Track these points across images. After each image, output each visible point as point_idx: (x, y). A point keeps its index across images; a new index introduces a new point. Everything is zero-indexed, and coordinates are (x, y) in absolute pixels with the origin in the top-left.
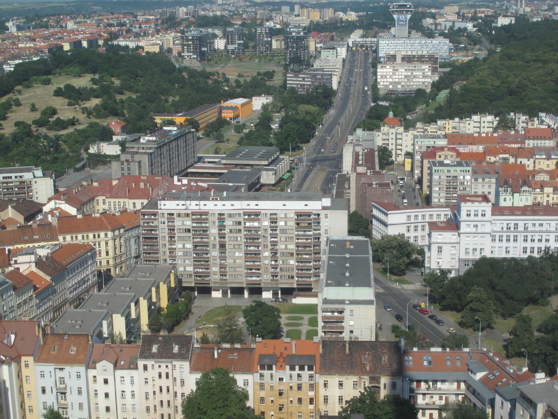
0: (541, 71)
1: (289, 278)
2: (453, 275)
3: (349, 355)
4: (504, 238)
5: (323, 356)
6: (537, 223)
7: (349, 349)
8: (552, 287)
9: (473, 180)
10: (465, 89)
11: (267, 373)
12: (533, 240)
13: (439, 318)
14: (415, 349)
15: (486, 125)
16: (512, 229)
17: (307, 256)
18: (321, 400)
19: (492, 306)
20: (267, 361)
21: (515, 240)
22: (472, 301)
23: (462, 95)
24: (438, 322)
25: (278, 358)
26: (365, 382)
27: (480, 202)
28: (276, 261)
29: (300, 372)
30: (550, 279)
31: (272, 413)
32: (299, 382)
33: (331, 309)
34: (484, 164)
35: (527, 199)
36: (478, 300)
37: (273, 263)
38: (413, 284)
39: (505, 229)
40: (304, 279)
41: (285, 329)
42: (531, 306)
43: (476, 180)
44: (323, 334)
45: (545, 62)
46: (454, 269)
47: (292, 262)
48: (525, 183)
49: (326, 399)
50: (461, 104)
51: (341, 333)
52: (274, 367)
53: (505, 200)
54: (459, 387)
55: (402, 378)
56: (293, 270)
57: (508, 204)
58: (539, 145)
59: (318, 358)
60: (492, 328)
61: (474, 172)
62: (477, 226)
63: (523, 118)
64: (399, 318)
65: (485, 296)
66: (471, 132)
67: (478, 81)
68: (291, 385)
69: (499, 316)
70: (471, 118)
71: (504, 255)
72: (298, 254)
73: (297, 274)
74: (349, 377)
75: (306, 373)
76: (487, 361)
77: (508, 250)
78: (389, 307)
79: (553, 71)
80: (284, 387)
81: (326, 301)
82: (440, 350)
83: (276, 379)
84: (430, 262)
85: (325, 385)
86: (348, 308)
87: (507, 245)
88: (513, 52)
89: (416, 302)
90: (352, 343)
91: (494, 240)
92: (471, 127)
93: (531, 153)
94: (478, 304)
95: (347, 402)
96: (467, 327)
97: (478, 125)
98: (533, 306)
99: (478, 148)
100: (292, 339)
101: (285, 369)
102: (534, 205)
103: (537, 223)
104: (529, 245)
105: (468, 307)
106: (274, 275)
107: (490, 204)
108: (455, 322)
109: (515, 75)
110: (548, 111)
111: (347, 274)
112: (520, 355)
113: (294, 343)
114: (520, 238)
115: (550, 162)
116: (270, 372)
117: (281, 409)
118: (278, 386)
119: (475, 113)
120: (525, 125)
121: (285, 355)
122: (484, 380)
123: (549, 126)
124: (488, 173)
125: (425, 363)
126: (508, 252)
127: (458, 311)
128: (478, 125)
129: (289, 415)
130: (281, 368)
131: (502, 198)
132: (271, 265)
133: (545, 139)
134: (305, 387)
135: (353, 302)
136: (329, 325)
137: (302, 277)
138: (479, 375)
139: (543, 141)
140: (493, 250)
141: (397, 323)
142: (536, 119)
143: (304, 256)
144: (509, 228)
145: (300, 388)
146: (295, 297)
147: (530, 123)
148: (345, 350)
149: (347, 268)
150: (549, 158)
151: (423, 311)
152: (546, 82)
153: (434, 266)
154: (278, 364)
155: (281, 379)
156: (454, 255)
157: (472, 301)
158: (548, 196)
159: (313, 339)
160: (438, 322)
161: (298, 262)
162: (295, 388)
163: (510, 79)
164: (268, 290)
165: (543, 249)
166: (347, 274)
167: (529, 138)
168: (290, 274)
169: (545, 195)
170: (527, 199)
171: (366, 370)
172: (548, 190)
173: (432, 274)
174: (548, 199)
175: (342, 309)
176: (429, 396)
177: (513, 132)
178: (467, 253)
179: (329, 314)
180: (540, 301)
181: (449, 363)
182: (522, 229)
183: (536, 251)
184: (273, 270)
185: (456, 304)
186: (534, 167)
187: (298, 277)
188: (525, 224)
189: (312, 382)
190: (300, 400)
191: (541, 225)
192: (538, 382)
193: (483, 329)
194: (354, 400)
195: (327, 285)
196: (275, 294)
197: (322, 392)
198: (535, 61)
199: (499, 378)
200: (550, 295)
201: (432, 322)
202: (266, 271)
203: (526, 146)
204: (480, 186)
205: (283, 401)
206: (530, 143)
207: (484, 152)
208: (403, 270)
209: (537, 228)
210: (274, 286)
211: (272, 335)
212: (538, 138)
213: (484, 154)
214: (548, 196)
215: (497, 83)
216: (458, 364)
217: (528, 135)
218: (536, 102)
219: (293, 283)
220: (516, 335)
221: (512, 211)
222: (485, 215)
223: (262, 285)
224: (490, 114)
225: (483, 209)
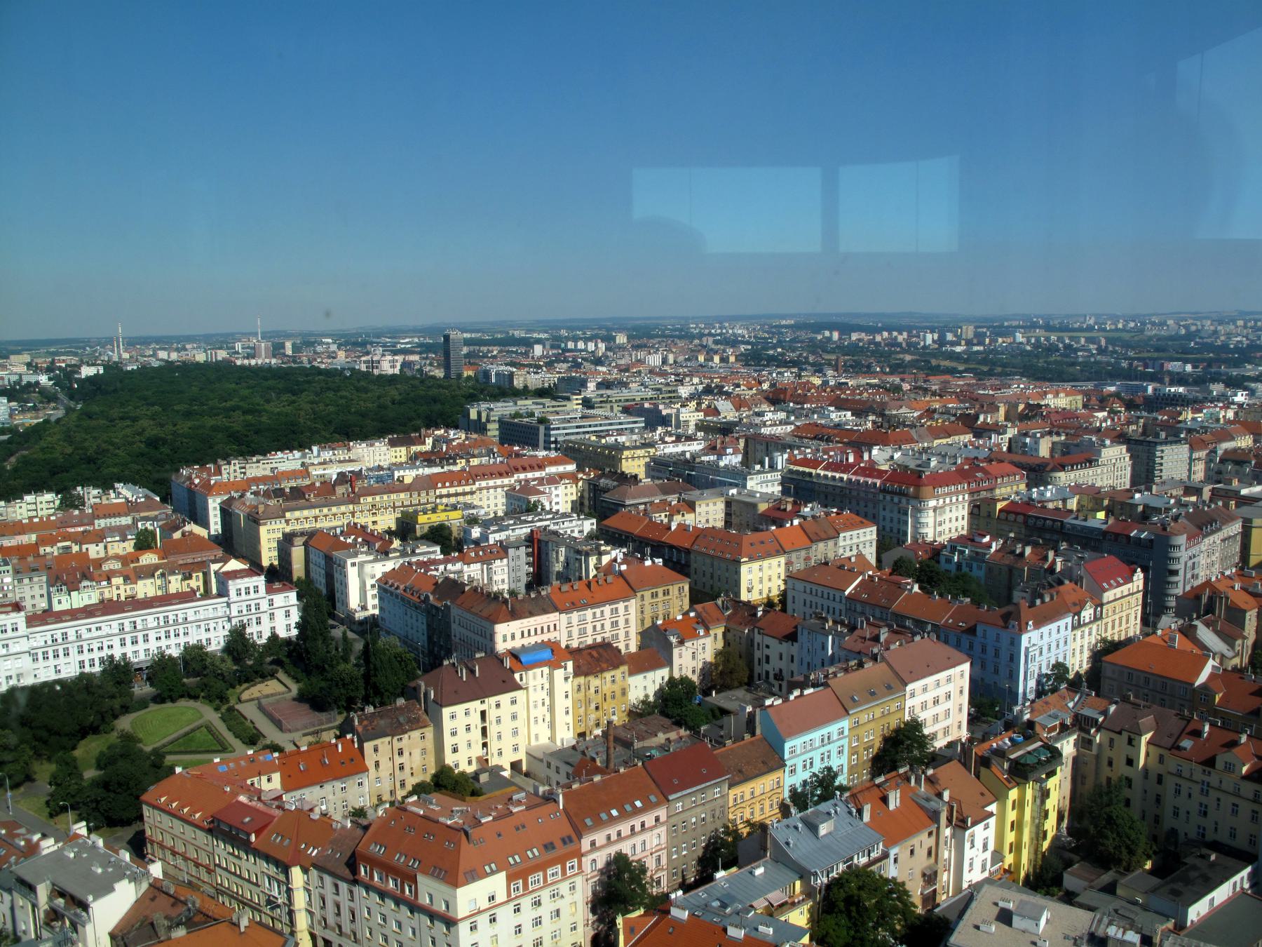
0: (128, 431)
4: (51, 655)
6: (93, 627)
9: (16, 582)
10: (25, 462)
12: (91, 650)
15: (45, 506)
16: (60, 641)
19: (28, 750)
21: (67, 654)
23: (15, 470)
27: (7, 613)
30: (113, 697)
34: (30, 559)
35: (90, 597)
39: (50, 642)
42: (89, 738)
43: (20, 581)
45: (135, 419)
48: (85, 576)
50: (11, 482)
53: (60, 602)
57: (65, 606)
58: (113, 524)
61: (17, 572)
62: (7, 646)
63: (95, 492)
66: (19, 517)
67: (42, 449)
69: (44, 762)
70: (22, 499)
71: (53, 676)
77: (58, 668)
79: (144, 430)
87: (56, 662)
88: (95, 408)
91: (35, 660)
92: (24, 510)
93: (99, 537)
97: (34, 507)
98: (94, 736)
99: (30, 539)
102: (102, 601)
103: (93, 627)
104: (86, 657)
107: (23, 614)
109: (95, 439)
110: (125, 480)
112: (64, 809)
114: (73, 651)
115: (126, 544)
119: (29, 493)
120: (98, 500)
123: (127, 499)
124: (37, 570)
128: (34, 507)
131: (55, 601)
133: (119, 515)
139: (118, 519)
140: (36, 672)
142: (111, 491)
144: (55, 640)
147: (104, 498)
150: (124, 540)
152: (134, 443)
158: (118, 588)
163: (86, 444)
167: (99, 518)
169: (114, 588)
170: (90, 597)
172: (118, 581)
174: (118, 592)
177: (77, 512)
180: (101, 728)
182: (74, 638)
183: (97, 662)
186: (106, 552)
188: (77, 632)
191: (99, 629)
192: (45, 852)
198: (122, 418)
200: (116, 717)
203: (97, 527)
204: (27, 589)
206: (101, 523)
207: (36, 543)
209: (95, 633)
212: (110, 516)
213: (37, 545)
214: (118, 588)
215: (69, 450)
217: (96, 513)
218: (115, 470)
220: (57, 785)
221: (60, 617)
222: (17, 629)
224: (50, 490)
225: (14, 621)
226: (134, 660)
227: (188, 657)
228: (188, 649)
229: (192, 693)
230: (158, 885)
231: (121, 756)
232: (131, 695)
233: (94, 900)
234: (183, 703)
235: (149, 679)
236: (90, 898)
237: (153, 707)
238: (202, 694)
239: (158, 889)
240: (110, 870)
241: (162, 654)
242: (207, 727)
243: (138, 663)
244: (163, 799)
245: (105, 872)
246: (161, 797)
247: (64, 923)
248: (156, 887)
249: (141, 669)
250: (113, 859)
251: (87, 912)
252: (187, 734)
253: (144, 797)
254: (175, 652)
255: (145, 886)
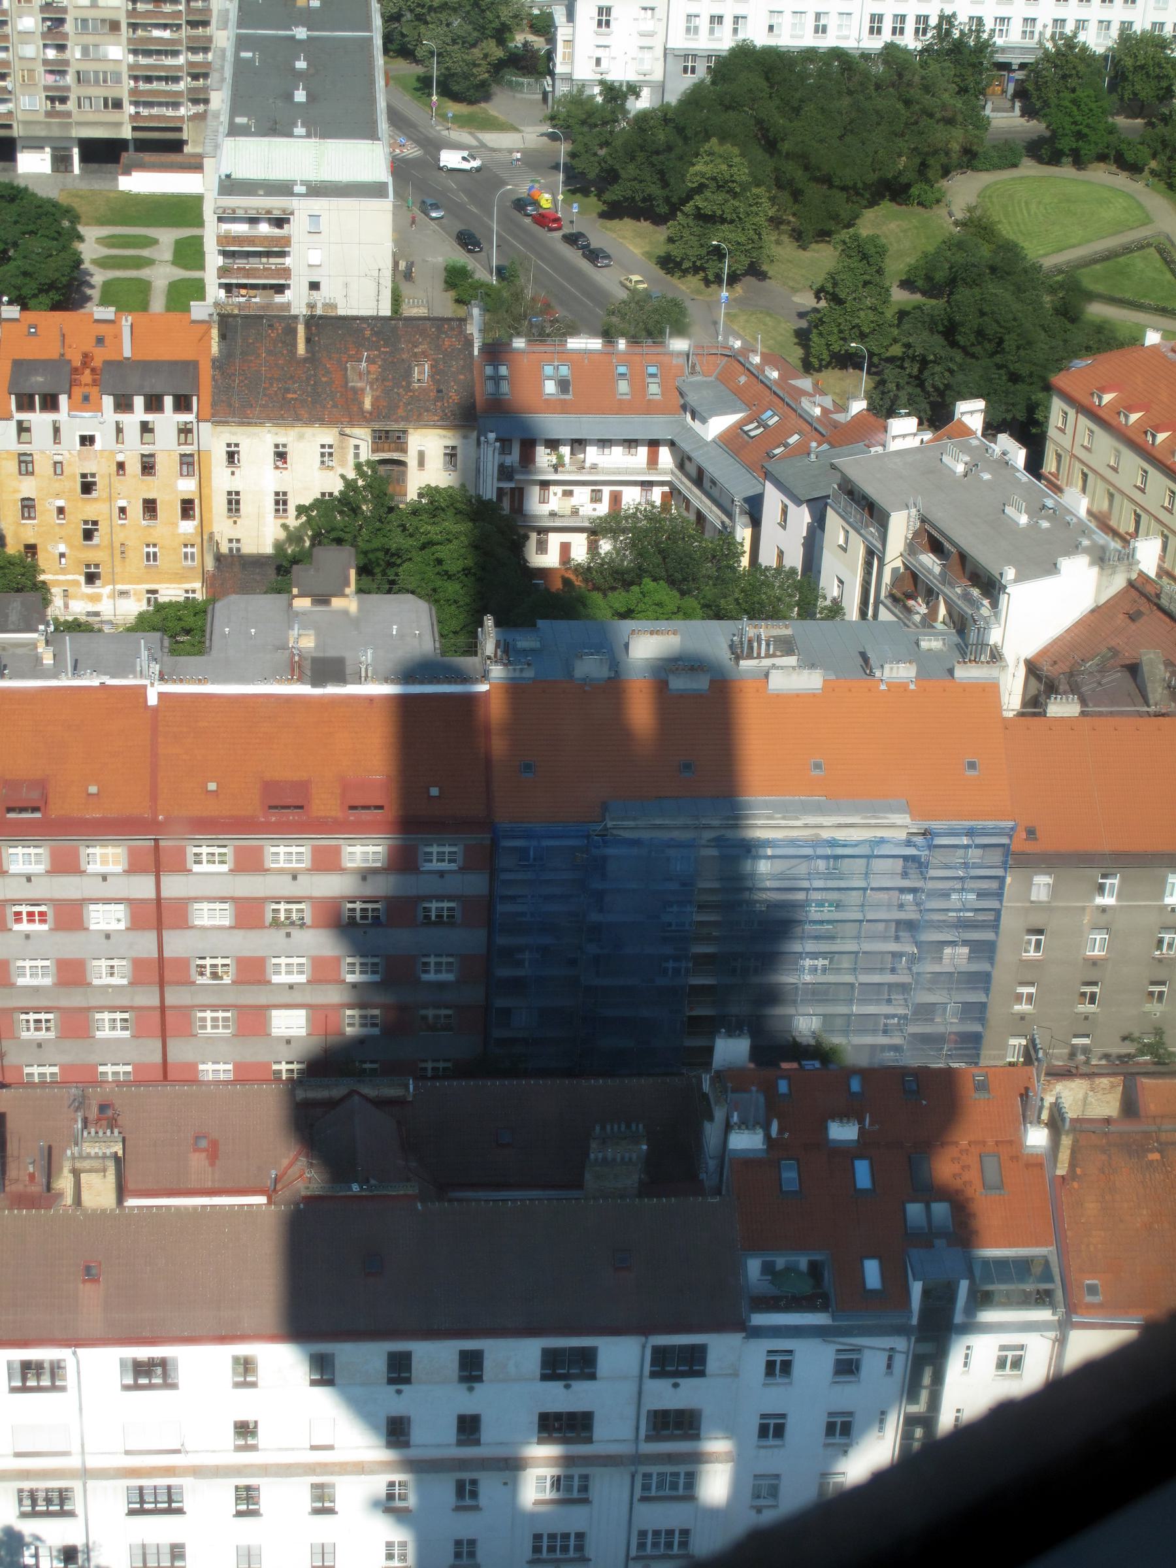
1: (106, 106)
2: (643, 103)
3: (305, 360)
5: (219, 365)
7: (308, 340)
8: (955, 147)
11: (39, 419)
13: (595, 243)
14: (519, 343)
17: (167, 34)
18: (219, 504)
19: (766, 204)
20: (38, 382)
22: (701, 188)
24: (593, 255)
25: (75, 370)
26: (357, 447)
28: (61, 48)
29: (149, 417)
30: (950, 122)
31: (62, 548)
32: (147, 449)
33: (246, 210)
36: (722, 185)
37: (51, 54)
38: (516, 130)
40: (155, 111)
41: (99, 277)
42: (887, 207)
44: (222, 293)
46: (647, 83)
47: (116, 52)
49: (234, 503)
51: (280, 289)
52: (63, 399)
54: (653, 461)
55: (475, 434)
56: (118, 80)
59: (206, 374)
60: (762, 276)
64: (468, 241)
65: (742, 173)
68: (120, 458)
69: (785, 238)
71: (808, 40)
72: (134, 26)
73: (134, 92)
74: (309, 431)
75: (168, 420)
76: (743, 379)
77: (823, 22)
78: (436, 207)
80: (97, 464)
81: (229, 186)
82: (596, 344)
83: (71, 439)
84: (570, 58)
85: (231, 456)
86: (302, 209)
89: (523, 191)
90: (316, 323)
94: (720, 197)
95: (301, 510)
96: (685, 272)
98: (894, 207)
100: (121, 308)
101: (98, 408)
105: (688, 208)
106: (57, 97)
108: (648, 255)
111: (300, 96)
112: (847, 361)
113: (126, 322)
116: (49, 417)
117: (88, 535)
118: (77, 462)
121: (97, 363)
122: (732, 441)
125: (550, 387)
126: (821, 29)
127: (659, 220)
129: (117, 552)
130: (87, 402)
132: (46, 62)
134: (166, 464)
135: (317, 190)
136: (240, 263)
137: (150, 105)
138: (717, 425)
141: (460, 257)
143: (156, 33)
145: (148, 467)
146: (127, 172)
148: (294, 345)
149: (300, 75)
151: (545, 220)
153: (584, 71)
154: (78, 392)
155: (87, 440)
156: (651, 35)
157: (701, 188)
159: (187, 309)
160: (593, 255)
161: (135, 52)
162: (134, 467)
164: (36, 144)
165: (933, 21)
166: (300, 96)
168: (111, 93)
171: (361, 409)
173: (578, 99)
175: (284, 211)
176: (559, 490)
178: (691, 30)
179: (241, 228)
180: (914, 191)
181: (623, 386)
184: (50, 79)
185: (649, 199)
187: (136, 104)
189: (187, 449)
190: (150, 507)
192: (895, 446)
193: (733, 279)
194: (324, 503)
195: (234, 131)
196: (61, 161)
197: (221, 480)
199: (776, 435)
200: (946, 172)
201: (574, 256)
202: (29, 82)
205: (92, 508)
208: (483, 85)
210: (56, 132)
211: (55, 296)
216: (654, 389)
219: (119, 125)
220: (836, 299)
223: (17, 131)
226: (999, 41)
227: (1129, 62)
228: (1126, 37)
229: (1130, 156)
230: (1149, 589)
231: (993, 269)
232: (982, 124)
233: (1017, 580)
234: (1102, 176)
235: (1021, 93)
236: (1010, 573)
237: (1029, 168)
238: (1153, 164)
239: (1142, 594)
240: (1045, 524)
241: (1070, 43)
242: (1161, 251)
243: (1003, 50)
244: (1107, 398)
245: (1033, 526)
246: (1103, 390)
247: (933, 612)
248: (1138, 588)
249: (1006, 66)
250: (1049, 503)
251: (995, 604)
252: (1109, 256)
253: (1059, 380)
254: (1097, 42)
255: (1118, 582)
